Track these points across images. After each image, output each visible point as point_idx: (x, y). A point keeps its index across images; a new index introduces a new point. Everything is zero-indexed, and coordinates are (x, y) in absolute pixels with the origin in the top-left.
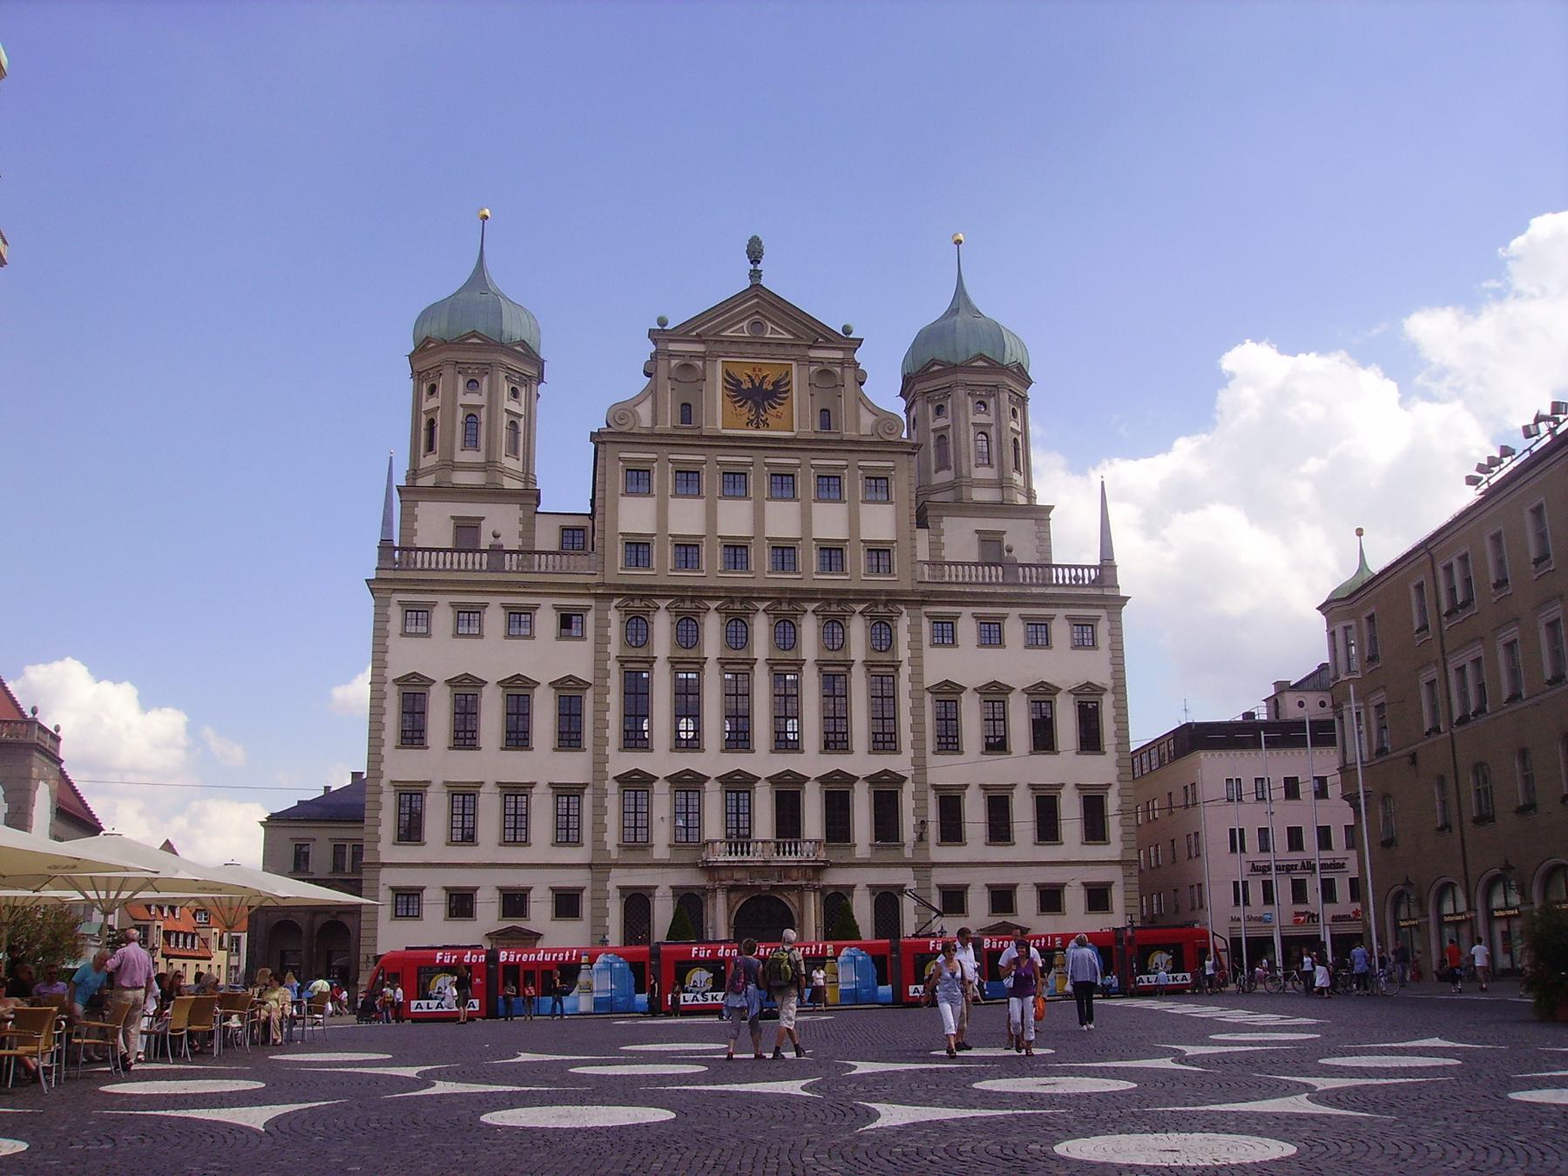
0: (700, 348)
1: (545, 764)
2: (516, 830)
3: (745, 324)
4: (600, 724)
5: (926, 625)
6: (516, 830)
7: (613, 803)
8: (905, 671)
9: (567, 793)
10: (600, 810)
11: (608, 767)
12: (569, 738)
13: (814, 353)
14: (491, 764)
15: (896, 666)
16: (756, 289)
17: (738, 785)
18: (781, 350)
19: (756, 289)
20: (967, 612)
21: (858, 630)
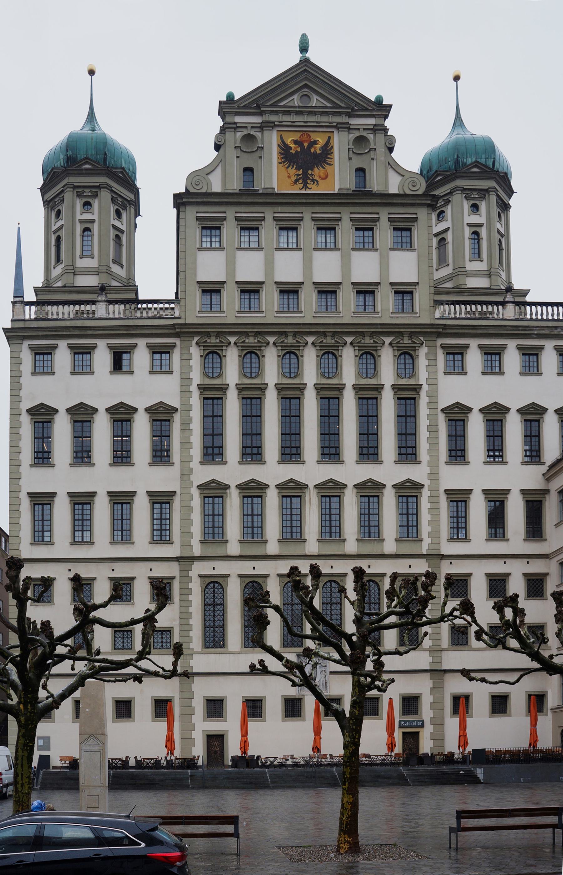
0: (257, 120)
1: (143, 477)
2: (122, 530)
3: (295, 97)
4: (186, 444)
5: (441, 356)
6: (122, 530)
7: (196, 502)
8: (423, 394)
9: (161, 500)
10: (187, 511)
11: (192, 478)
12: (161, 455)
13: (354, 122)
14: (102, 477)
15: (417, 389)
16: (305, 62)
17: (292, 491)
18: (324, 119)
19: (305, 62)
20: (474, 343)
21: (387, 361)
